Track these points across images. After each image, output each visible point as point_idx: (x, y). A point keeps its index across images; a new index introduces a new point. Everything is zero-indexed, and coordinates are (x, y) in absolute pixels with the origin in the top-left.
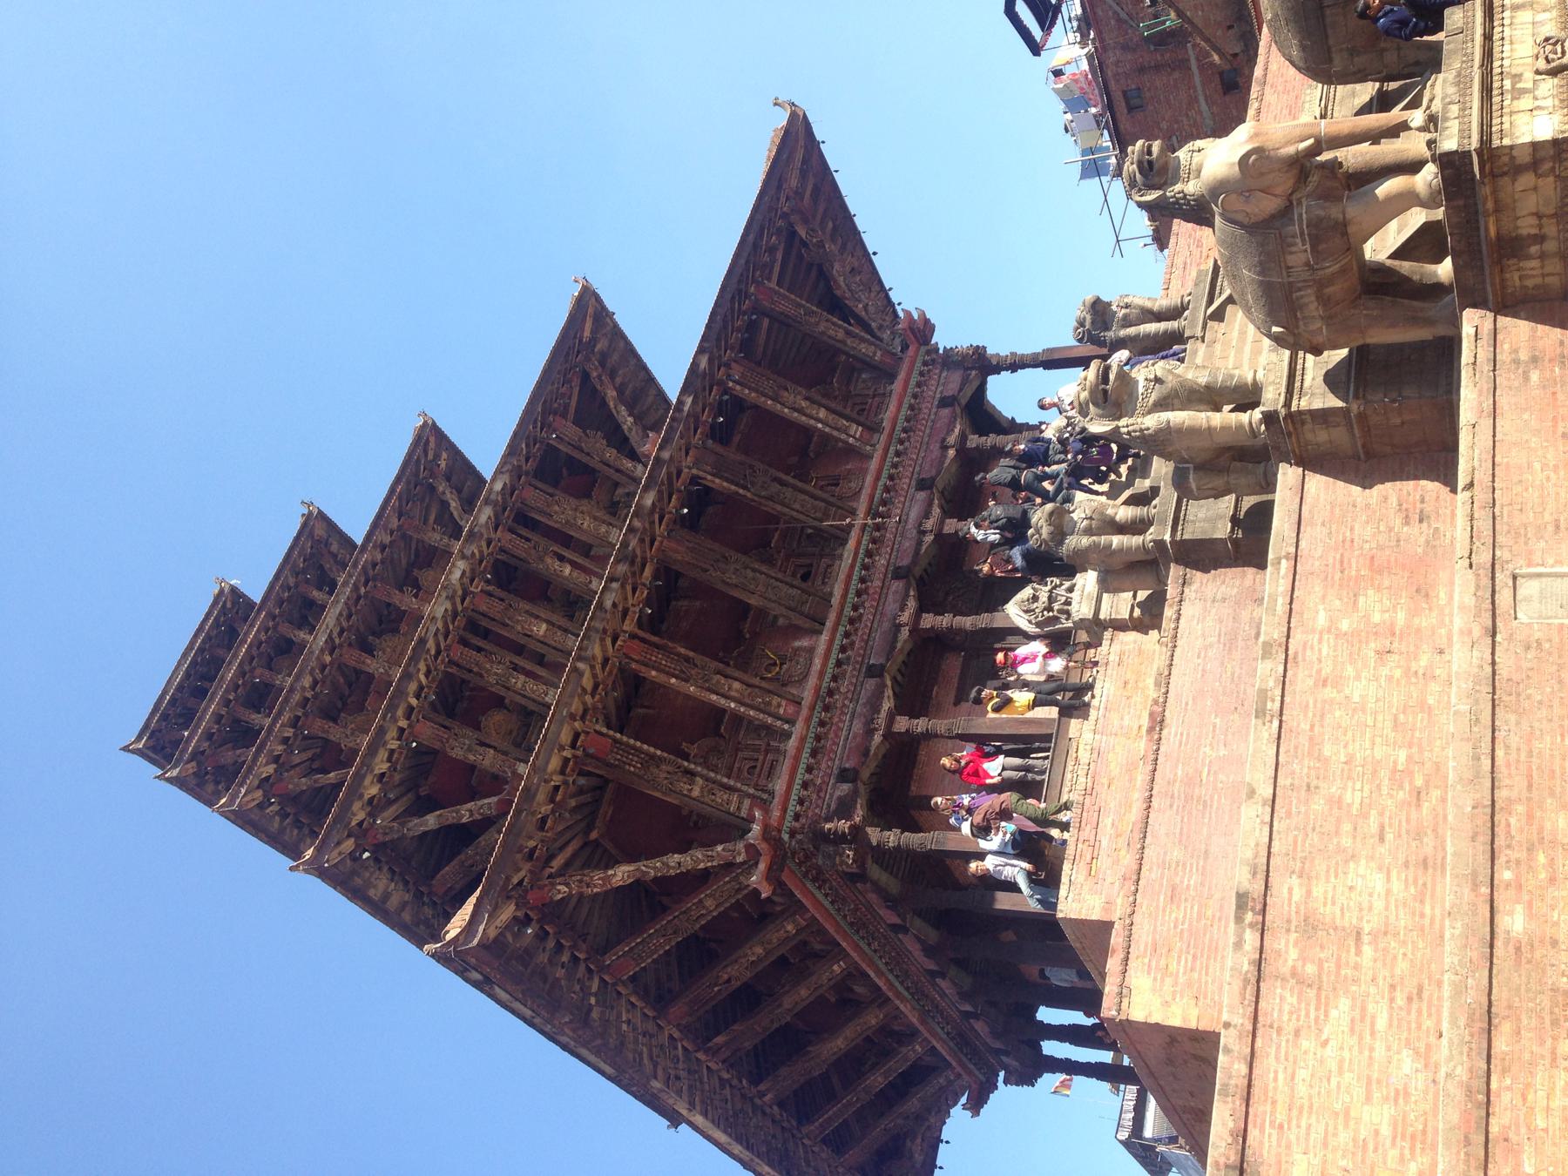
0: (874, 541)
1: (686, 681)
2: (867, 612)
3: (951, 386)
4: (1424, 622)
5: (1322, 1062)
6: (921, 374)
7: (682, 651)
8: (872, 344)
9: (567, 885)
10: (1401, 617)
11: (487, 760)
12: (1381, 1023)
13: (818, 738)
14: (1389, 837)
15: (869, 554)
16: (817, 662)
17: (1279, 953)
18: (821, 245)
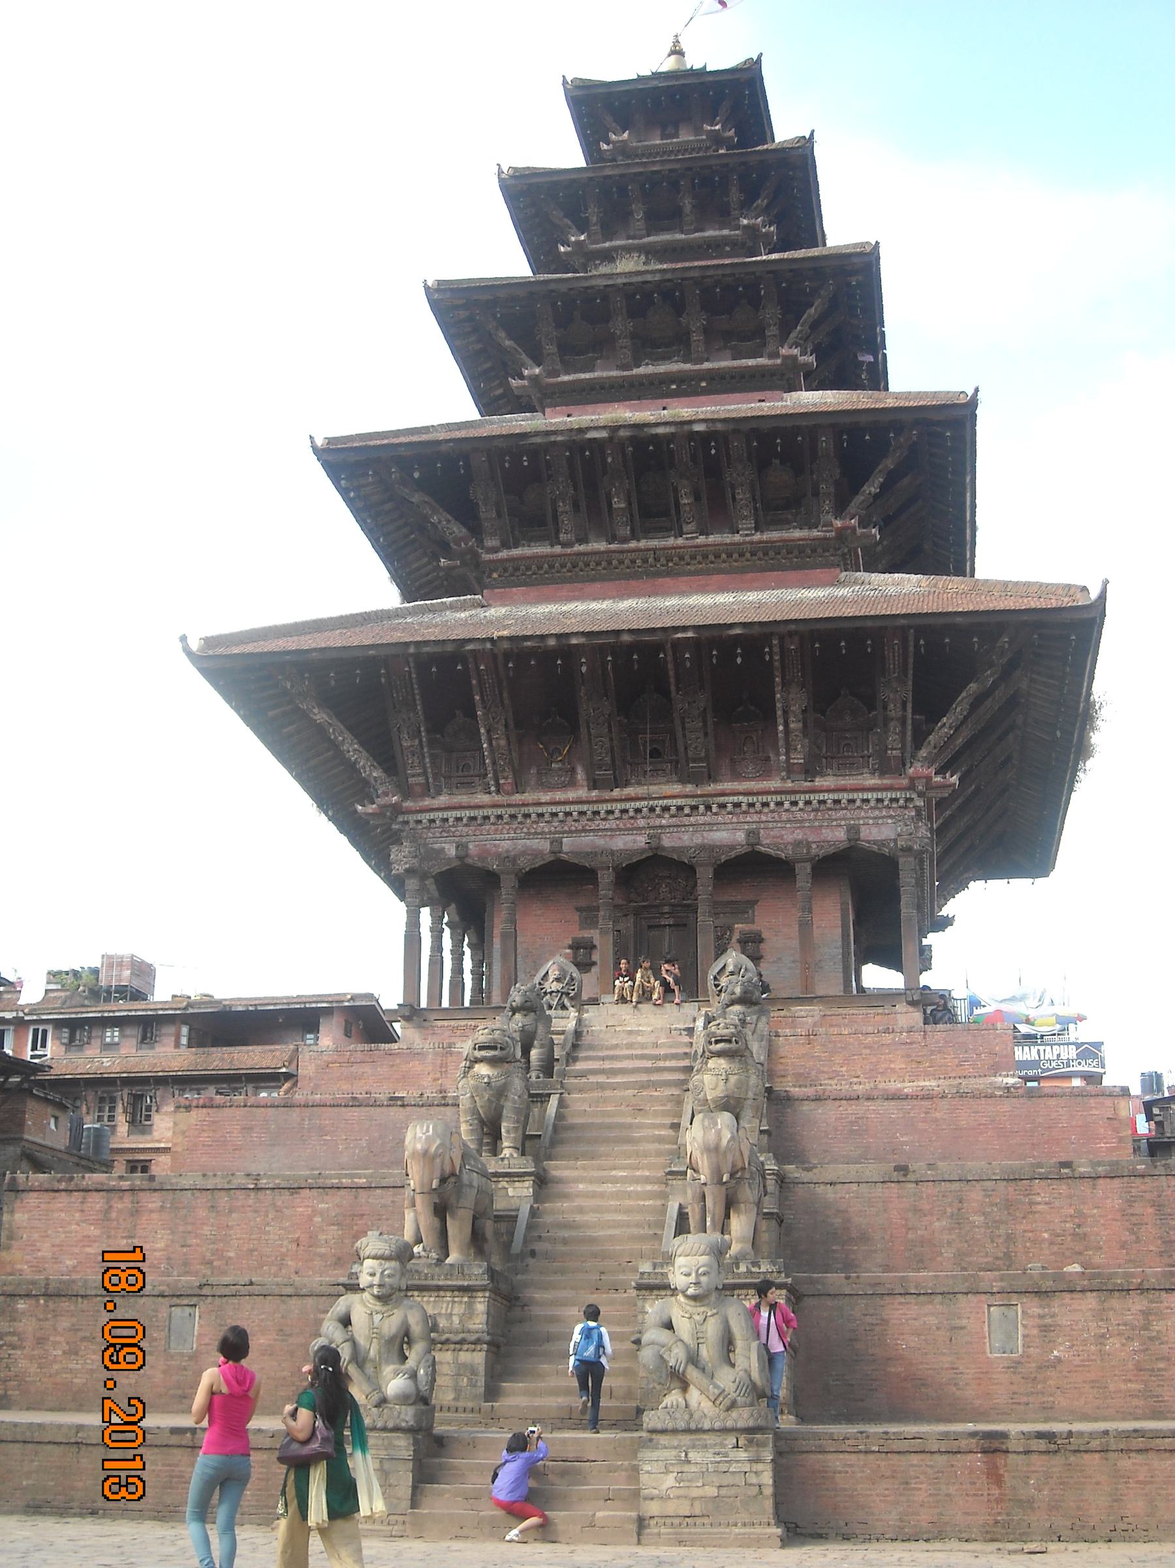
0: (680, 808)
1: (485, 708)
2: (611, 824)
3: (874, 830)
4: (317, 1263)
5: (70, 1224)
6: (879, 801)
7: (505, 695)
8: (903, 741)
9: (292, 686)
10: (323, 1250)
11: (487, 513)
12: (88, 1250)
13: (486, 818)
14: (185, 1250)
15: (666, 809)
16: (545, 797)
17: (121, 1198)
18: (991, 665)
